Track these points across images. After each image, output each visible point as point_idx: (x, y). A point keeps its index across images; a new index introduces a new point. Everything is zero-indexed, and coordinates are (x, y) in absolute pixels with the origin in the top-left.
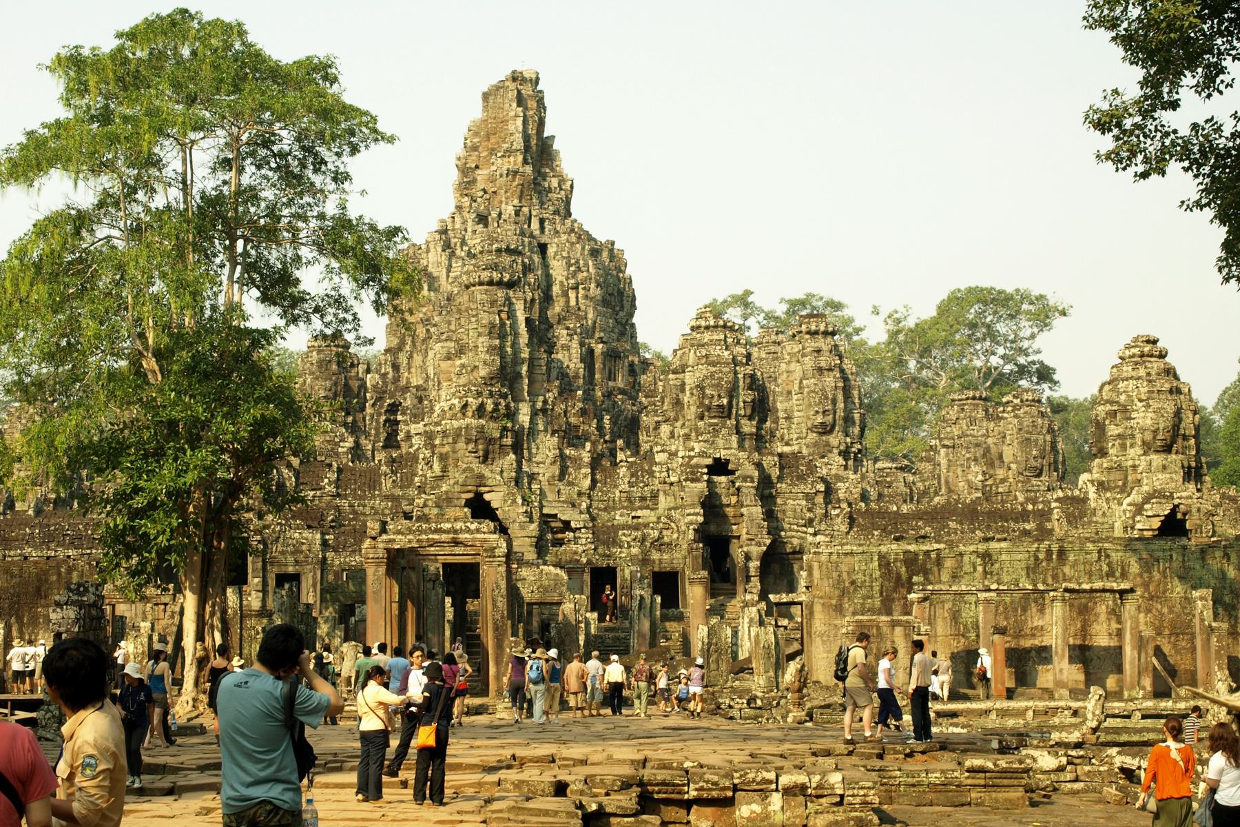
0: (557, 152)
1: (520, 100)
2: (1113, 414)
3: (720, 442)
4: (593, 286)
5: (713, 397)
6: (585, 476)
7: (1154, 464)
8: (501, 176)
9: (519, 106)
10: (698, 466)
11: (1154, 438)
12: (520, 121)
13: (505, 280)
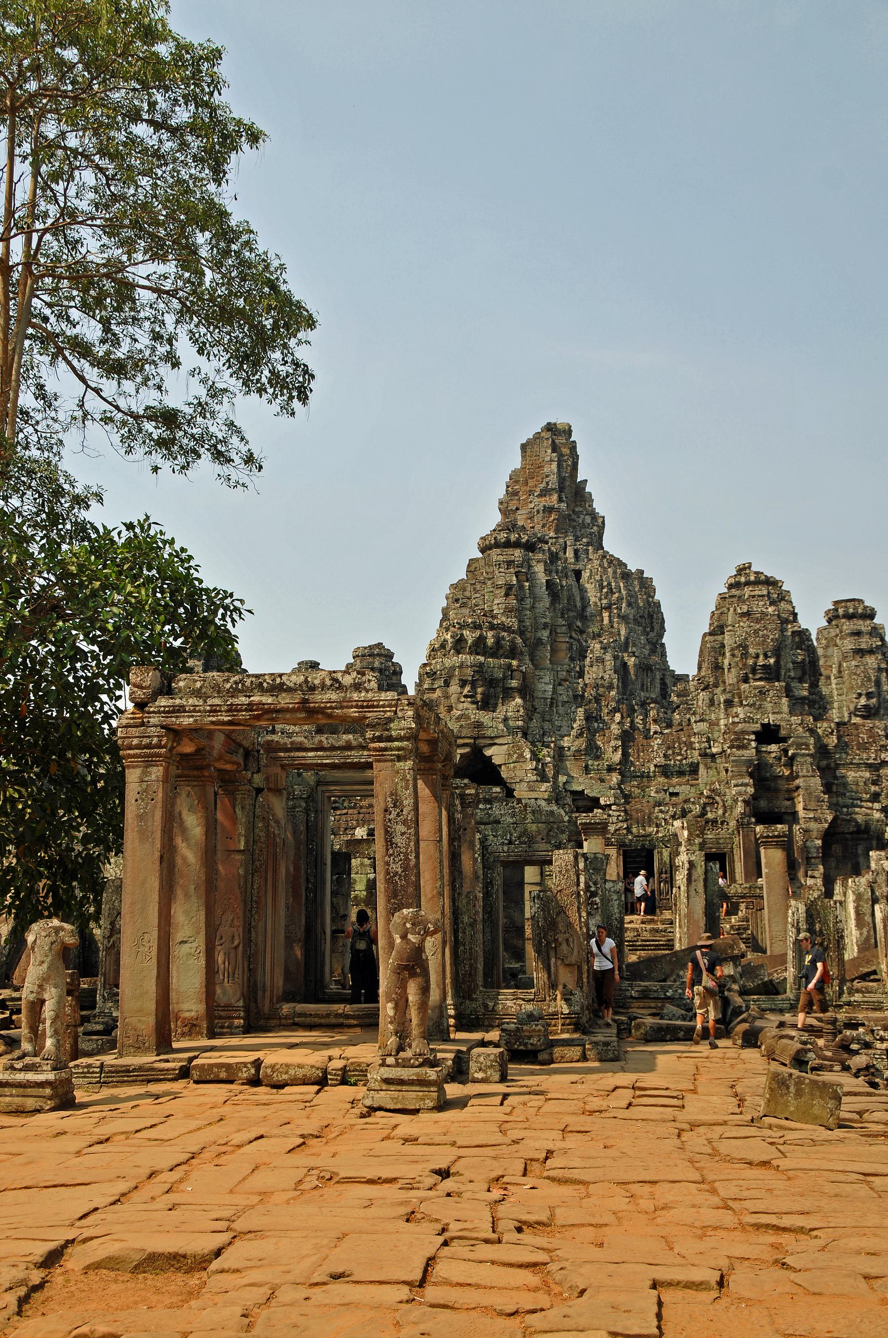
0: (590, 494)
1: (555, 448)
3: (769, 706)
4: (624, 605)
5: (757, 656)
6: (615, 749)
8: (538, 512)
9: (554, 451)
10: (744, 732)
12: (554, 466)
13: (524, 540)
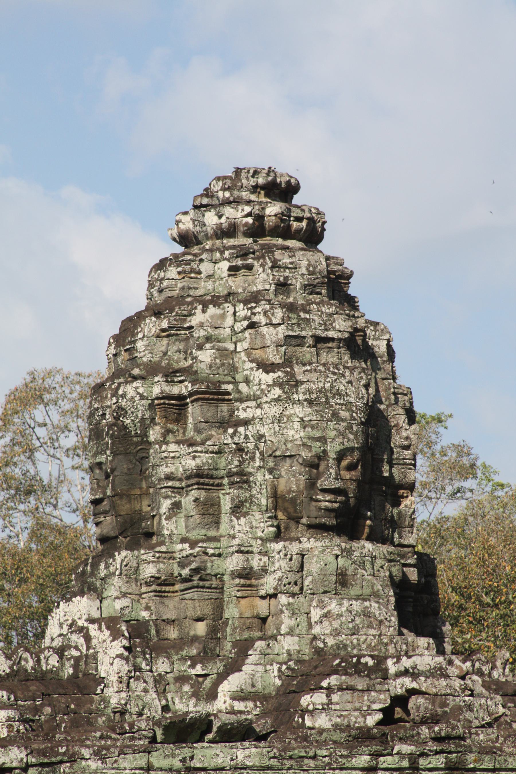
2: (174, 408)
7: (313, 566)
11: (311, 484)
